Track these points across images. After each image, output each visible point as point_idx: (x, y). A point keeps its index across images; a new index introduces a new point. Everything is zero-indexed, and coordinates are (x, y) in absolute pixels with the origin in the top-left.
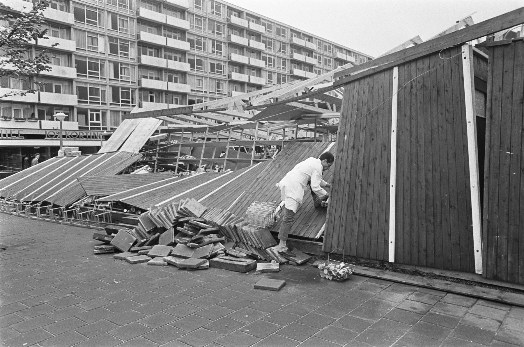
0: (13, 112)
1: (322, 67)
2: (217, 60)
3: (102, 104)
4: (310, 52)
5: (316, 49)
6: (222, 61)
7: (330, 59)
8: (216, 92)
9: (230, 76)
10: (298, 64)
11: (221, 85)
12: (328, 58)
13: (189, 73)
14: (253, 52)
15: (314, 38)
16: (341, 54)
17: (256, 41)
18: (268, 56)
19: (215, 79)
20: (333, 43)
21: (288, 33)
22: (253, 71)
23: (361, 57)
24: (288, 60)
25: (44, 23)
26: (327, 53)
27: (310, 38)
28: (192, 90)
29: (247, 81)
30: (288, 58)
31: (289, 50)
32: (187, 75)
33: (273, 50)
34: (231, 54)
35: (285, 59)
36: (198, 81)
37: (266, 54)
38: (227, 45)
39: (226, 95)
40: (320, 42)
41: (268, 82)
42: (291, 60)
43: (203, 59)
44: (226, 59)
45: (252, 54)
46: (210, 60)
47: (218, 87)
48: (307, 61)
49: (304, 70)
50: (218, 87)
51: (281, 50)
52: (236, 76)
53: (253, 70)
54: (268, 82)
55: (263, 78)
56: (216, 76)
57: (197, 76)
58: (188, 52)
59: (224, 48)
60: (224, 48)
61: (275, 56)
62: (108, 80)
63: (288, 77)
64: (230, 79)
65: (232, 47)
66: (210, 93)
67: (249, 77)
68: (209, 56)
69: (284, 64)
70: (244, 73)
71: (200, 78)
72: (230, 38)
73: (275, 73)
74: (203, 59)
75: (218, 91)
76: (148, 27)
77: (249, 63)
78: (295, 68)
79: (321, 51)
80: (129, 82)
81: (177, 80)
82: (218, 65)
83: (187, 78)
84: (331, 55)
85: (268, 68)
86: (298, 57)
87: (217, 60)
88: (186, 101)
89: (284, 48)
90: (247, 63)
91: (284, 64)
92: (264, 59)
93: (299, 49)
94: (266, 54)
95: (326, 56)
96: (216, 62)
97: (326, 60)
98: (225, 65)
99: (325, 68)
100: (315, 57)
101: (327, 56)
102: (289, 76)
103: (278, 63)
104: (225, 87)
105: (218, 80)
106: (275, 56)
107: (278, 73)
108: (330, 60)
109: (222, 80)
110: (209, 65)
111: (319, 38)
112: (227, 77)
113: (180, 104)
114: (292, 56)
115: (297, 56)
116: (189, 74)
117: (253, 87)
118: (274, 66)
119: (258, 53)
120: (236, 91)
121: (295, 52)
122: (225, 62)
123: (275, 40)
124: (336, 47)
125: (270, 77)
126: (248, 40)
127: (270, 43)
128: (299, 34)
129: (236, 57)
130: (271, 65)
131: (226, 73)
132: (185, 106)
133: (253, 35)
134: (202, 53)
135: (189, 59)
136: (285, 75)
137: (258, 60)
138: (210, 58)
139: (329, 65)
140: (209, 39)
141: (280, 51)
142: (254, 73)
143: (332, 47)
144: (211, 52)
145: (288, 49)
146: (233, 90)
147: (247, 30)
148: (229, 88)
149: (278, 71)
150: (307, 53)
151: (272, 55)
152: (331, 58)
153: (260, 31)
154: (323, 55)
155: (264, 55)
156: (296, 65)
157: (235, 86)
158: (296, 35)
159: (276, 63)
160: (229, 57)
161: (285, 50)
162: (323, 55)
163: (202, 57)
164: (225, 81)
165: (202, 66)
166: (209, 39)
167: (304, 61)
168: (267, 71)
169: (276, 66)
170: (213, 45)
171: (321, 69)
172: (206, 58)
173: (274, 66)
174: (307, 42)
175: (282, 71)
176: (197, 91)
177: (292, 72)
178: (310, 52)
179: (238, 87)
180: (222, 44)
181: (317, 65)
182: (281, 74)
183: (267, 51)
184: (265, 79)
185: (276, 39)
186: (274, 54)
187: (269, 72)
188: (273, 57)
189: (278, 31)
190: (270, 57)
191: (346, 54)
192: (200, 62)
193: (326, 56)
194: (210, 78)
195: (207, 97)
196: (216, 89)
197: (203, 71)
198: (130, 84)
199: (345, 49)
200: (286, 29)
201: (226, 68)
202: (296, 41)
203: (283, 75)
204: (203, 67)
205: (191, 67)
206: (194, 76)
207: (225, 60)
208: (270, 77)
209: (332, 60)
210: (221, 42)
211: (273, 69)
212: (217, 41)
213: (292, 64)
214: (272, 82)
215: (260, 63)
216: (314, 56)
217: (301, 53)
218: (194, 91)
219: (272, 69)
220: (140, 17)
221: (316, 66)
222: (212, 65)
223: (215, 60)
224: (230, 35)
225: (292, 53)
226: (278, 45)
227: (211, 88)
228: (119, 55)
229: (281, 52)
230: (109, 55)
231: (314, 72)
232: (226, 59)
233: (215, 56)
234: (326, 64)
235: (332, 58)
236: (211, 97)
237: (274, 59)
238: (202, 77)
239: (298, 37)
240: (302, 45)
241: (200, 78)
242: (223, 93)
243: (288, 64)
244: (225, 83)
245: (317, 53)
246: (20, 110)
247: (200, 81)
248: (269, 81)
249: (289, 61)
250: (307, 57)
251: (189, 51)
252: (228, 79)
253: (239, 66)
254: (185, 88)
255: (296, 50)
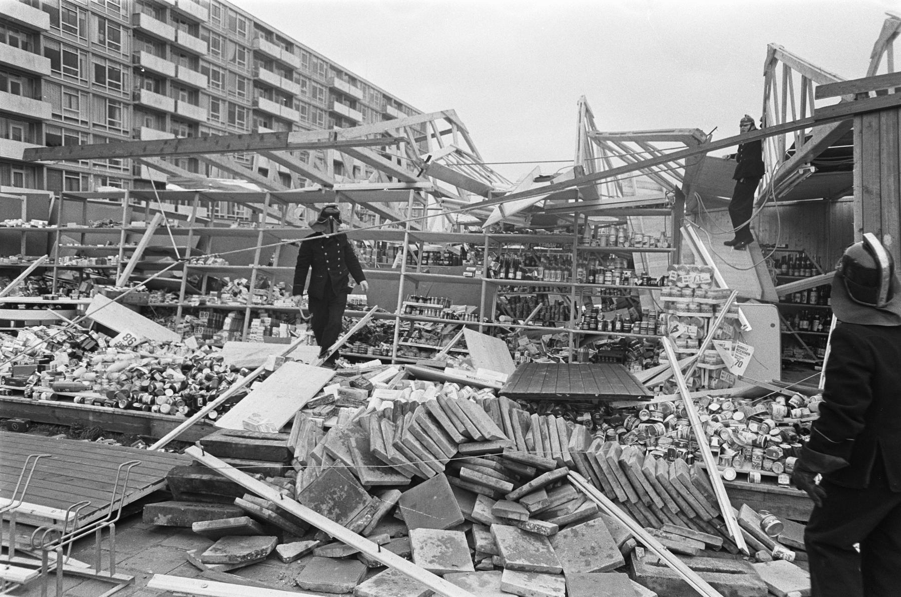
0: (12, 176)
1: (306, 100)
2: (110, 60)
3: (124, 170)
4: (288, 71)
5: (206, 19)
6: (120, 64)
7: (304, 79)
8: (107, 125)
9: (136, 97)
10: (266, 90)
11: (117, 111)
12: (319, 86)
13: (48, 78)
14: (182, 56)
15: (297, 46)
16: (341, 81)
17: (189, 33)
18: (211, 67)
19: (105, 99)
20: (327, 61)
21: (249, 28)
22: (181, 93)
23: (372, 91)
24: (249, 79)
25: (356, 146)
26: (316, 77)
27: (289, 45)
28: (54, 115)
29: (172, 110)
30: (249, 76)
31: (252, 63)
32: (43, 82)
33: (222, 56)
34: (139, 52)
35: (244, 78)
36: (68, 97)
37: (209, 63)
38: (131, 33)
39: (127, 132)
40: (307, 54)
41: (210, 118)
42: (135, 30)
43: (79, 54)
44: (128, 61)
45: (181, 58)
46: (94, 57)
47: (112, 115)
48: (283, 87)
49: (277, 102)
50: (112, 115)
51: (237, 60)
52: (148, 98)
53: (182, 90)
54: (210, 118)
55: (202, 107)
56: (107, 92)
57: (65, 86)
58: (45, 33)
59: (125, 37)
60: (125, 37)
61: (225, 69)
62: (91, 125)
63: (248, 112)
64: (137, 102)
65: (142, 40)
66: (94, 125)
67: (176, 103)
68: (92, 48)
69: (241, 86)
70: (164, 94)
71: (73, 93)
72: (139, 19)
73: (224, 101)
74: (79, 54)
75: (111, 123)
76: (146, 44)
77: (176, 76)
78: (261, 96)
79: (307, 72)
80: (120, 130)
81: (19, 89)
82: (111, 70)
83: (43, 87)
84: (323, 81)
85: (211, 90)
86: (265, 75)
87: (110, 60)
88: (41, 135)
89: (242, 57)
90: (173, 74)
91: (241, 86)
92: (205, 72)
93: (269, 62)
94: (209, 63)
95: (315, 81)
96: (107, 65)
97: (315, 88)
98: (126, 72)
99: (313, 102)
100: (297, 82)
101: (317, 83)
102: (249, 109)
103: (231, 85)
104: (125, 116)
105: (111, 101)
106: (225, 69)
107: (230, 103)
108: (321, 91)
109: (120, 103)
110: (93, 67)
111: (243, 13)
112: (130, 98)
113: (25, 141)
114: (257, 74)
115: (265, 75)
116: (46, 80)
117: (182, 123)
118: (223, 87)
119: (193, 59)
120: (147, 126)
121: (261, 66)
122: (126, 67)
123: (226, 38)
124: (333, 68)
125: (215, 108)
126: (174, 29)
127: (216, 44)
128: (269, 34)
129: (149, 60)
130: (218, 86)
131: (129, 90)
132: (40, 146)
133: (184, 23)
134: (78, 42)
135: (46, 48)
136: (243, 108)
137: (193, 72)
138: (93, 54)
139: (319, 99)
140: (93, 13)
141: (234, 60)
142: (183, 96)
143: (325, 67)
144: (96, 42)
145: (249, 57)
146: (143, 125)
147: (172, 10)
148: (135, 120)
149: (230, 98)
150: (283, 72)
151: (219, 67)
152: (322, 86)
153: (199, 16)
154: (310, 79)
155: (205, 65)
156: (263, 91)
157: (146, 117)
158: (263, 34)
159: (226, 82)
160: (136, 59)
161: (244, 61)
162: (310, 79)
163: (76, 49)
164: (126, 105)
165: (120, 81)
166: (93, 13)
167: (278, 85)
168: (209, 95)
169: (228, 88)
170: (101, 27)
171: (306, 103)
172: (85, 52)
173: (223, 87)
174: (284, 51)
175: (237, 100)
176: (66, 118)
177: (255, 103)
178: (288, 71)
179: (152, 119)
180: (121, 30)
181: (300, 97)
182: (235, 105)
183: (210, 58)
184: (205, 111)
185: (227, 36)
186: (223, 64)
187: (214, 98)
188: (221, 72)
189: (232, 22)
190: (216, 69)
191: (349, 83)
192: (71, 60)
193: (315, 81)
194: (94, 95)
195: (88, 134)
196: (108, 119)
197: (79, 77)
198: (122, 134)
199: (346, 74)
200: (247, 22)
201: (128, 80)
202: (265, 46)
203: (240, 106)
204: (121, 84)
205: (52, 67)
206: (60, 85)
207: (126, 63)
208: (215, 108)
209: (324, 90)
210: (119, 25)
211: (220, 93)
212: (110, 21)
213: (256, 90)
214: (218, 117)
215: (198, 80)
216: (296, 79)
217: (272, 71)
218: (60, 117)
219: (219, 93)
220: (141, 28)
221: (298, 97)
222: (99, 70)
223: (105, 59)
224: (139, 14)
225: (257, 68)
226: (231, 50)
227: (95, 118)
228: (236, 125)
229: (237, 64)
230: (93, 84)
231: (294, 108)
232: (128, 61)
233: (107, 52)
234: (314, 96)
235: (326, 87)
236: (95, 132)
237: (223, 75)
238: (77, 90)
239: (267, 39)
240: (274, 55)
241: (73, 93)
242: (122, 129)
243: (249, 87)
244: (125, 109)
245: (300, 74)
246: (22, 174)
247: (73, 100)
248: (213, 116)
249: (251, 83)
250: (284, 79)
251: (46, 31)
252: (132, 102)
253: (155, 80)
254: (41, 110)
255: (263, 63)
